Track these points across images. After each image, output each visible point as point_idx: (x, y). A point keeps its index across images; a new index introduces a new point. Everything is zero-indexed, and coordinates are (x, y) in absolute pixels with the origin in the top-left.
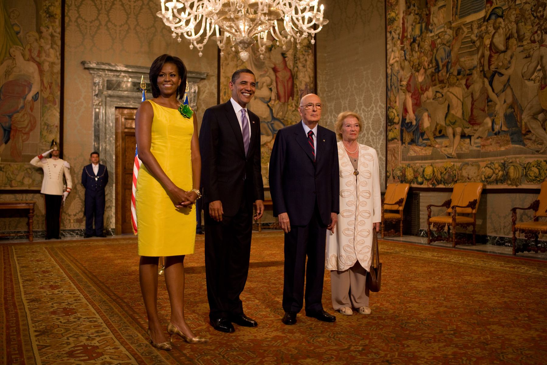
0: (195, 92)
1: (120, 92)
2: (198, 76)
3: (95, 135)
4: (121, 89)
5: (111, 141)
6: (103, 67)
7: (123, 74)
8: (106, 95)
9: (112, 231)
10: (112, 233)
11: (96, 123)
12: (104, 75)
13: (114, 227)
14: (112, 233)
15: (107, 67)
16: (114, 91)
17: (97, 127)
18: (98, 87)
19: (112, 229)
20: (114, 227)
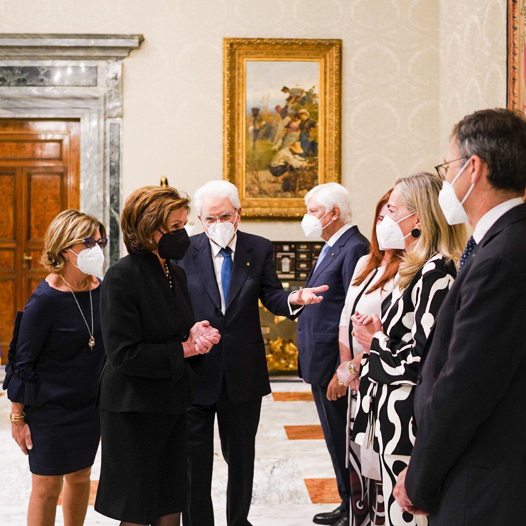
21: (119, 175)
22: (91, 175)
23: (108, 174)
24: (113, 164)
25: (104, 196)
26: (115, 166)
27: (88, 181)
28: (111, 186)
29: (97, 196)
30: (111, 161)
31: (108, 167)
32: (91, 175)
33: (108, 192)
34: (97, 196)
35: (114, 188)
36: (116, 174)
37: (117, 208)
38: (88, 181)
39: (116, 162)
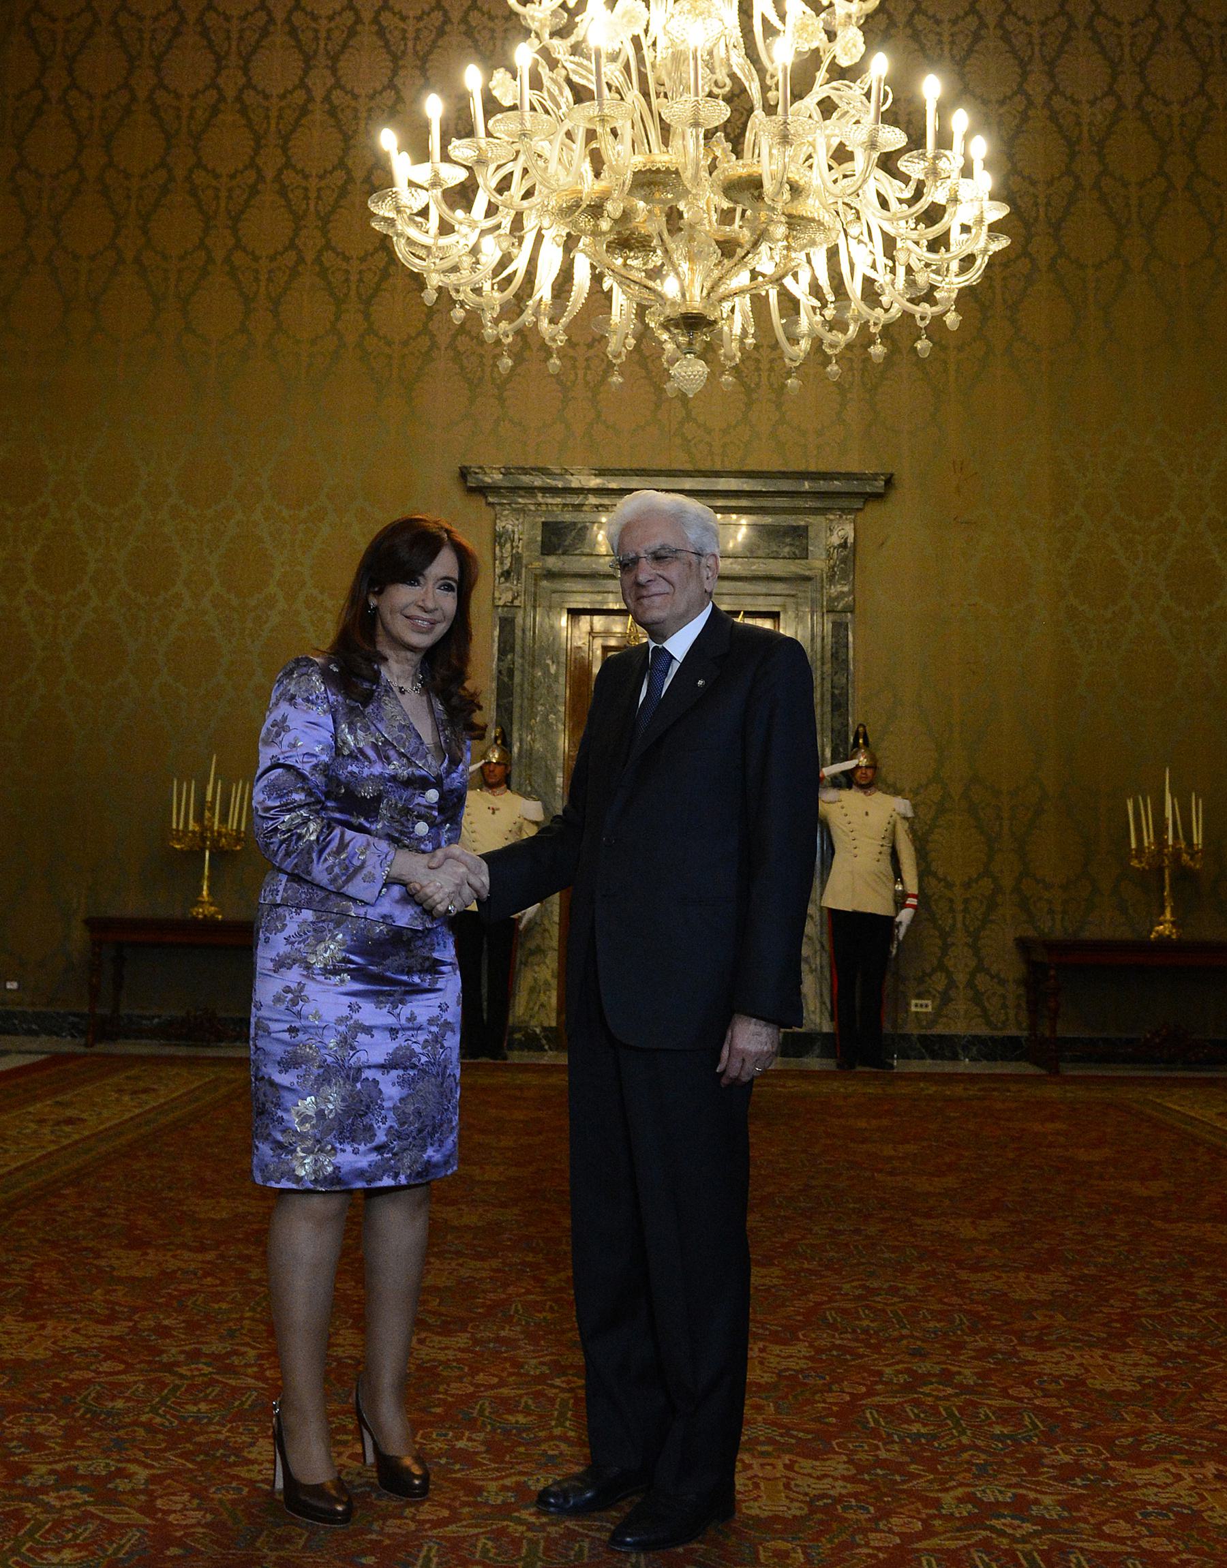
0: (844, 545)
1: (584, 559)
2: (854, 486)
3: (498, 706)
4: (587, 550)
6: (526, 480)
7: (593, 500)
8: (538, 572)
9: (546, 1037)
10: (544, 1042)
11: (505, 665)
12: (532, 508)
13: (554, 1024)
15: (538, 482)
16: (565, 558)
17: (506, 679)
18: (508, 545)
19: (544, 1029)
20: (554, 1024)
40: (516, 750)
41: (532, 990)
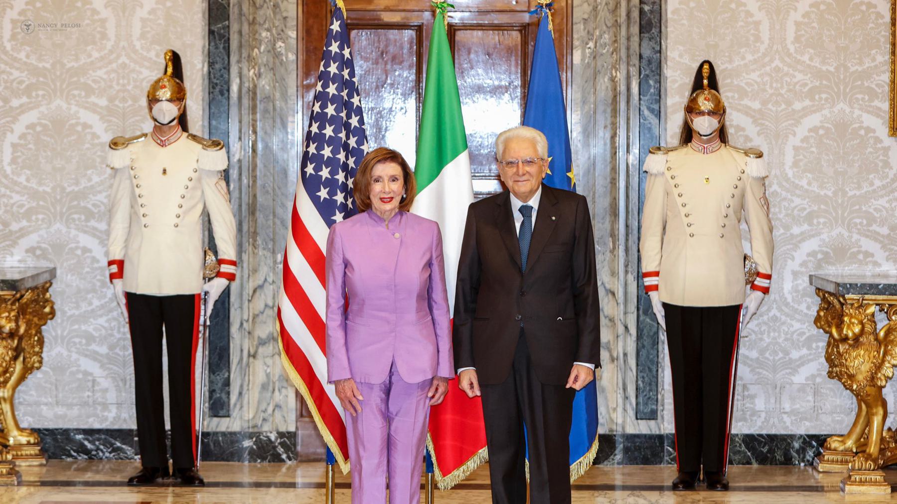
5: (277, 55)
10: (280, 450)
14: (280, 450)
19: (281, 435)
21: (660, 31)
22: (597, 33)
23: (635, 29)
24: (646, 8)
25: (628, 78)
26: (651, 12)
27: (591, 44)
28: (641, 57)
29: (613, 79)
30: (641, 2)
31: (636, 14)
32: (597, 33)
33: (634, 71)
34: (613, 79)
35: (650, 62)
36: (653, 31)
37: (656, 107)
38: (591, 44)
39: (654, 3)
40: (234, 88)
41: (264, 387)
